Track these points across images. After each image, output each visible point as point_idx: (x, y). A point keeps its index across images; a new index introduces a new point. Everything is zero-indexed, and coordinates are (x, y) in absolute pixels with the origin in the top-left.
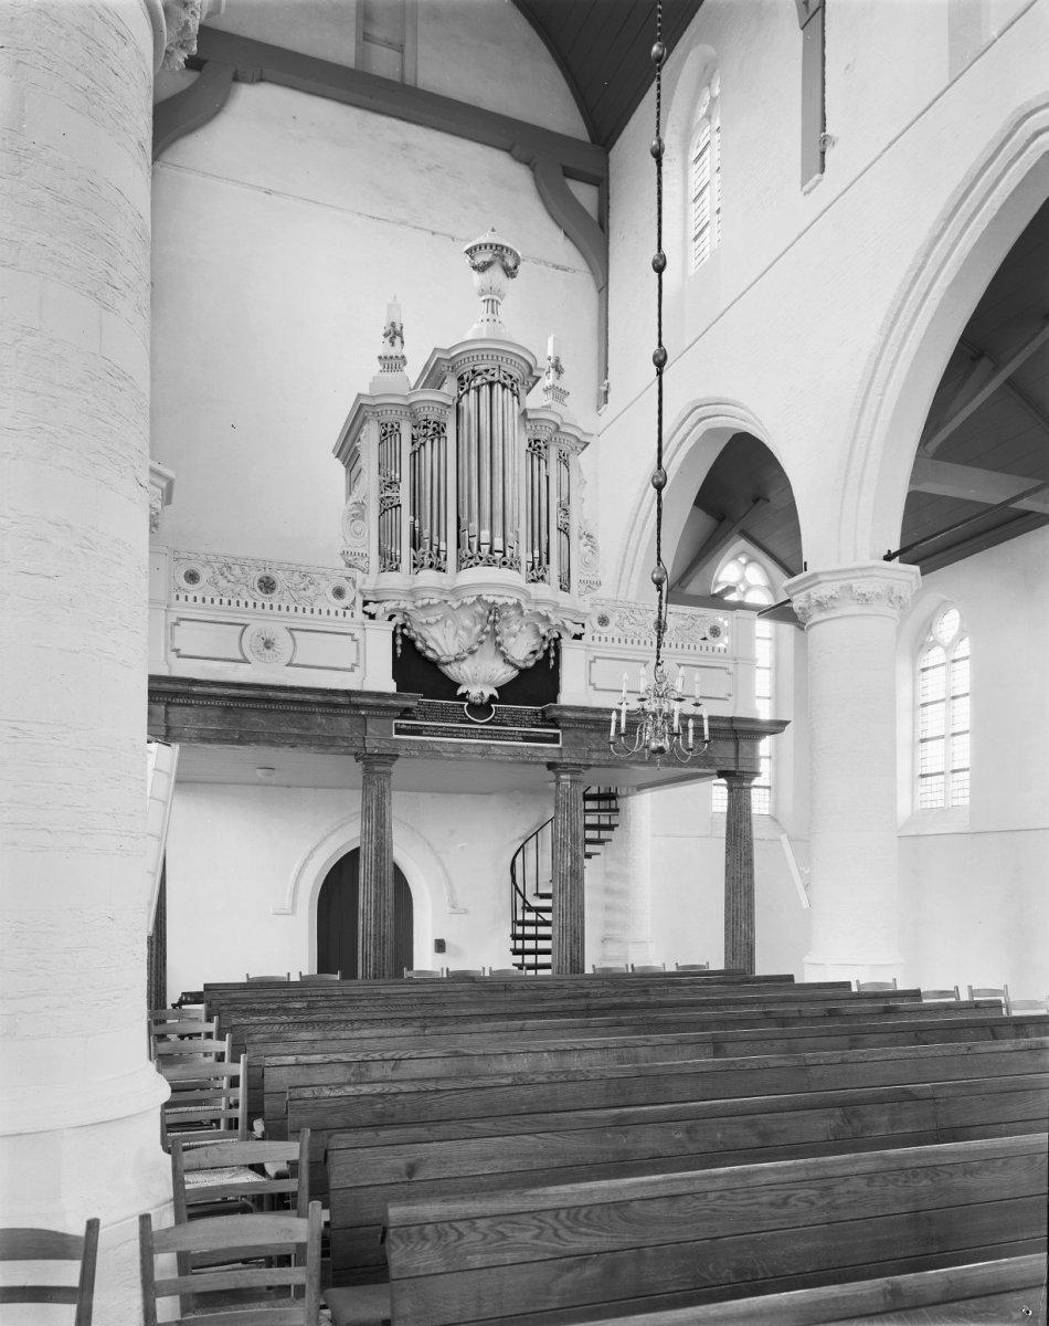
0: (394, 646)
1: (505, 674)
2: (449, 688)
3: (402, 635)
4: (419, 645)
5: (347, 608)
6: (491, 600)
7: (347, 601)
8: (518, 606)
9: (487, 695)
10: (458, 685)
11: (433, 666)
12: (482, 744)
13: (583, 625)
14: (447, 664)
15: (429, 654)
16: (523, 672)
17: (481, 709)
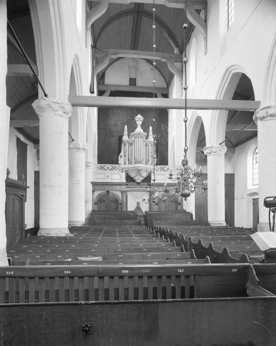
1: (143, 179)
4: (129, 175)
6: (138, 169)
7: (119, 169)
8: (142, 169)
11: (132, 178)
15: (131, 176)
16: (145, 178)
17: (138, 184)
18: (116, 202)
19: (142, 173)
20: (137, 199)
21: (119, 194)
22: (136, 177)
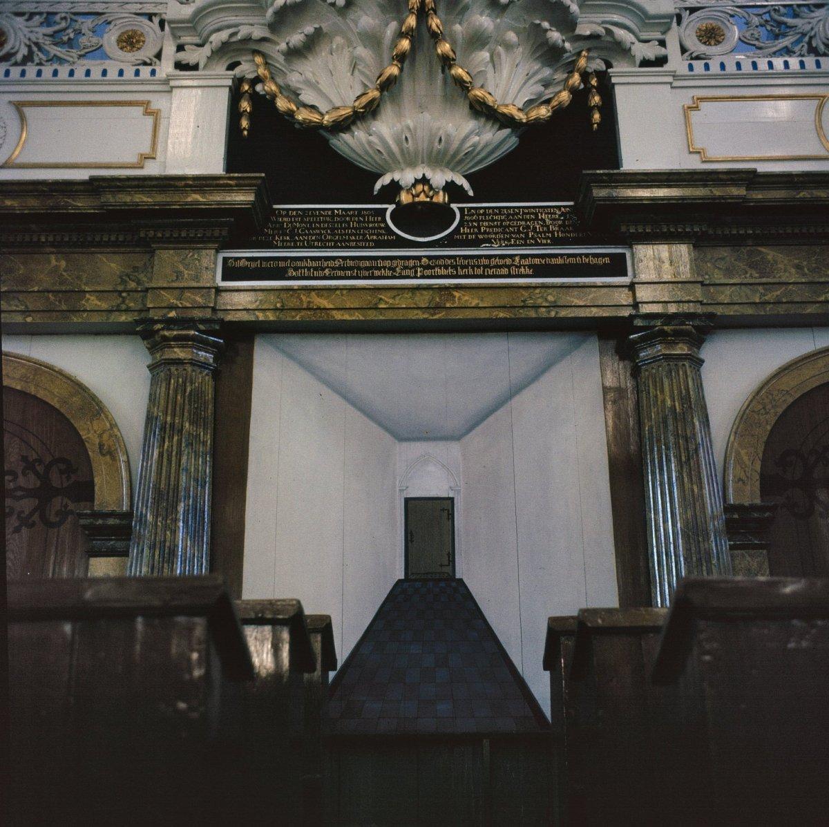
0: (234, 114)
2: (356, 180)
3: (255, 98)
4: (282, 104)
5: (145, 64)
7: (147, 53)
9: (439, 178)
10: (379, 176)
12: (429, 288)
13: (662, 43)
14: (343, 125)
16: (528, 132)
18: (57, 503)
19: (478, 40)
20: (418, 448)
21: (113, 377)
22: (388, 112)
